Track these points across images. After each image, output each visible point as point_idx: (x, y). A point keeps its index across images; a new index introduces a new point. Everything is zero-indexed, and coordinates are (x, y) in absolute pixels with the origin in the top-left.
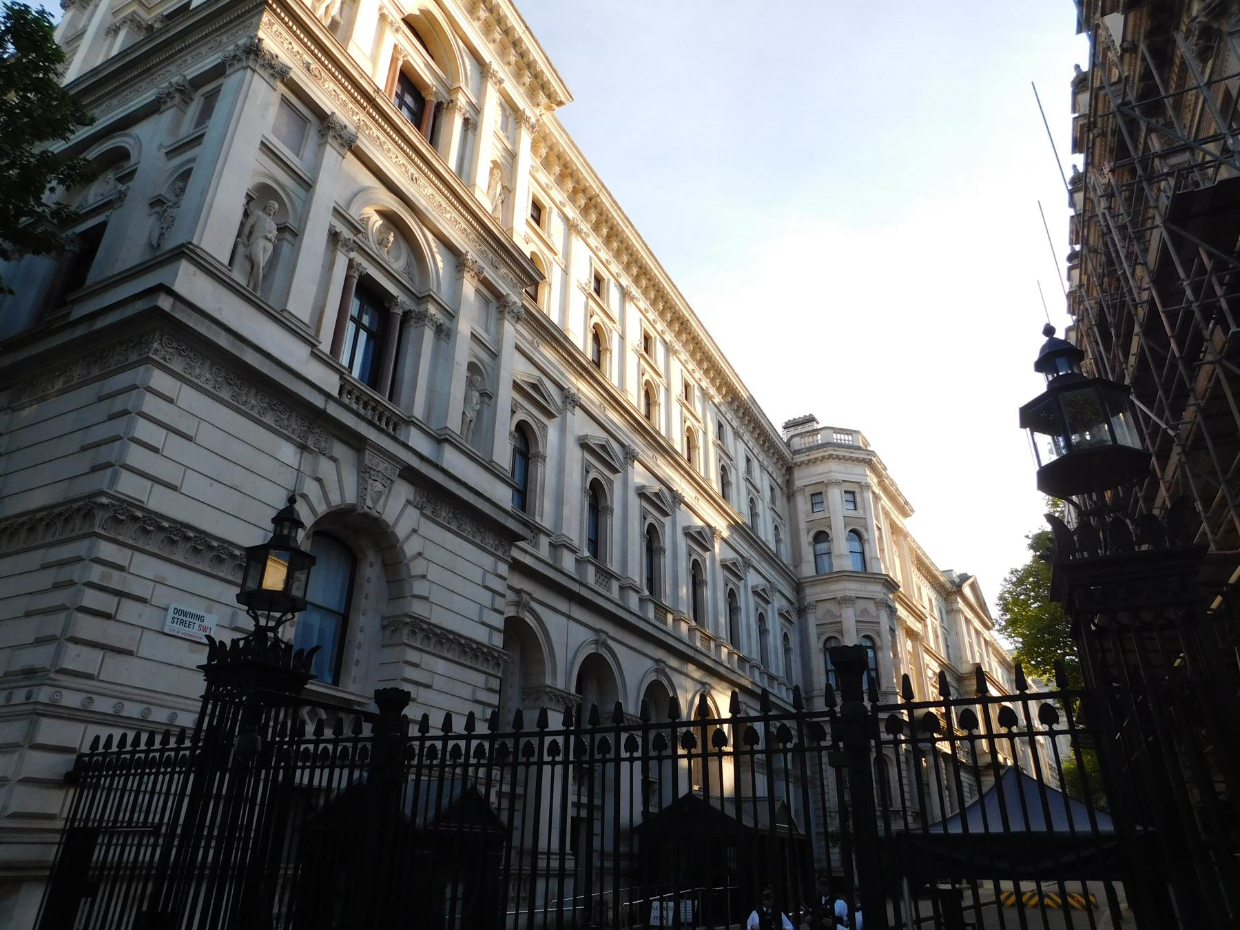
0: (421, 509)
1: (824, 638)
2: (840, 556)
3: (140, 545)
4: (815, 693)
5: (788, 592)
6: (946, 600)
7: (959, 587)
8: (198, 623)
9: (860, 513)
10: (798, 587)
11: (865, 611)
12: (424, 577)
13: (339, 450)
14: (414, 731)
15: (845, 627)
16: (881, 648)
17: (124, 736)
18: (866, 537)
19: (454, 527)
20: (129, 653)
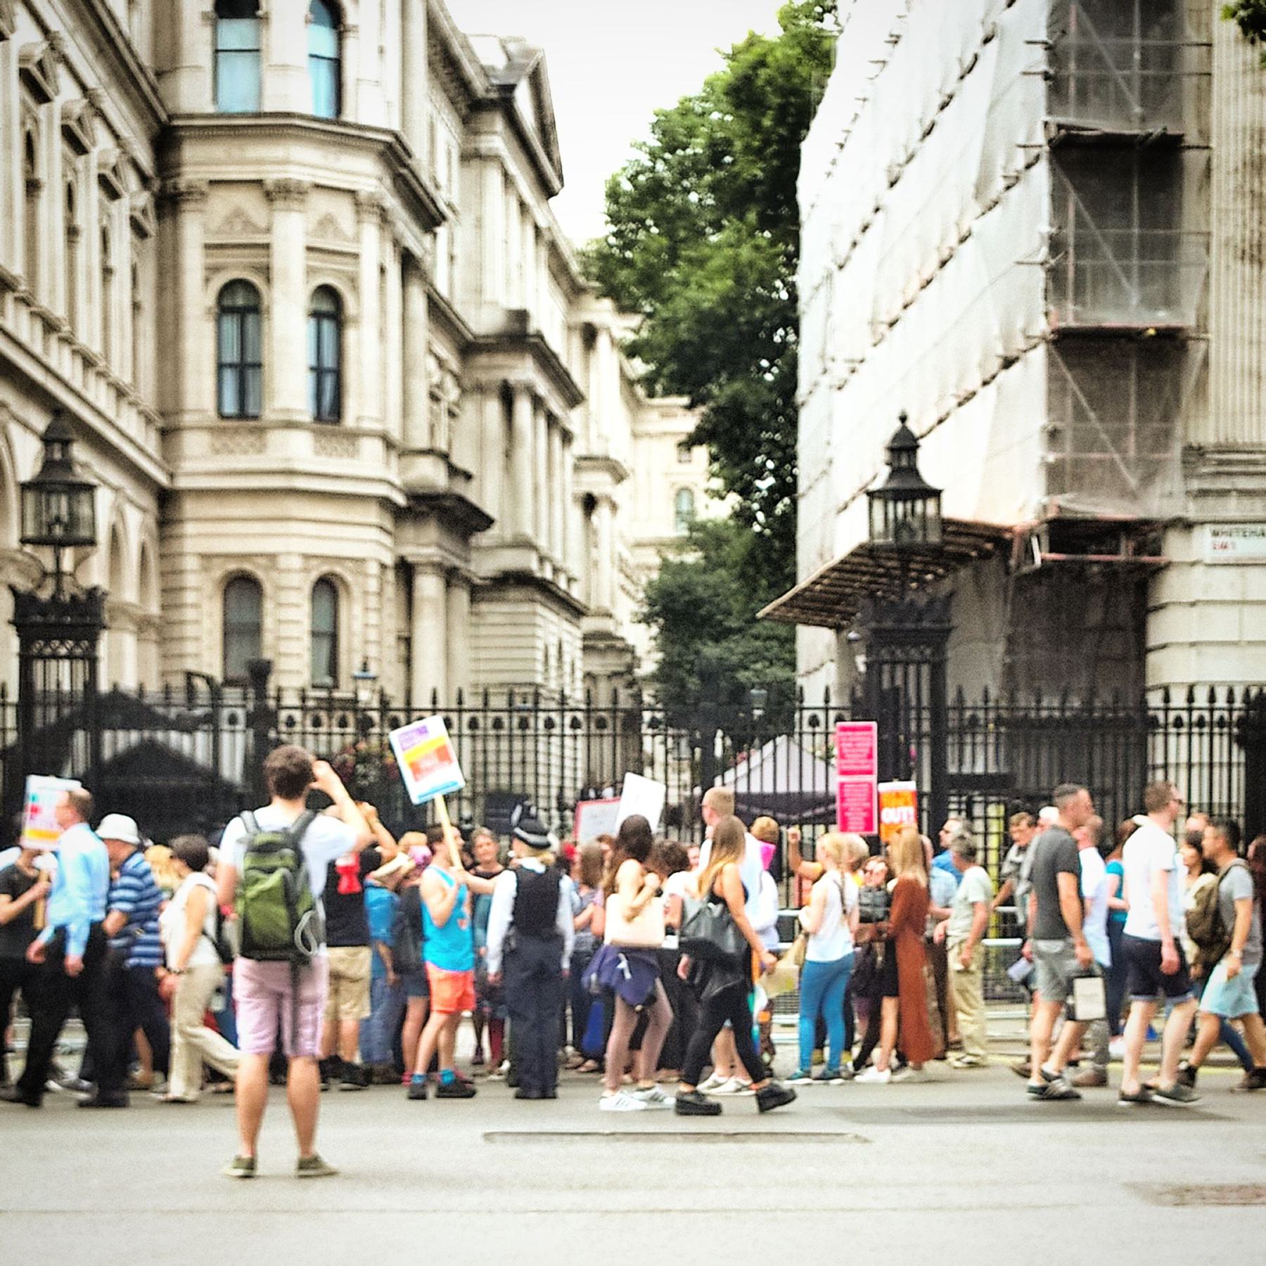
1: (220, 281)
4: (188, 419)
5: (145, 158)
6: (465, 121)
7: (511, 88)
10: (166, 138)
11: (327, 222)
15: (277, 263)
16: (356, 321)
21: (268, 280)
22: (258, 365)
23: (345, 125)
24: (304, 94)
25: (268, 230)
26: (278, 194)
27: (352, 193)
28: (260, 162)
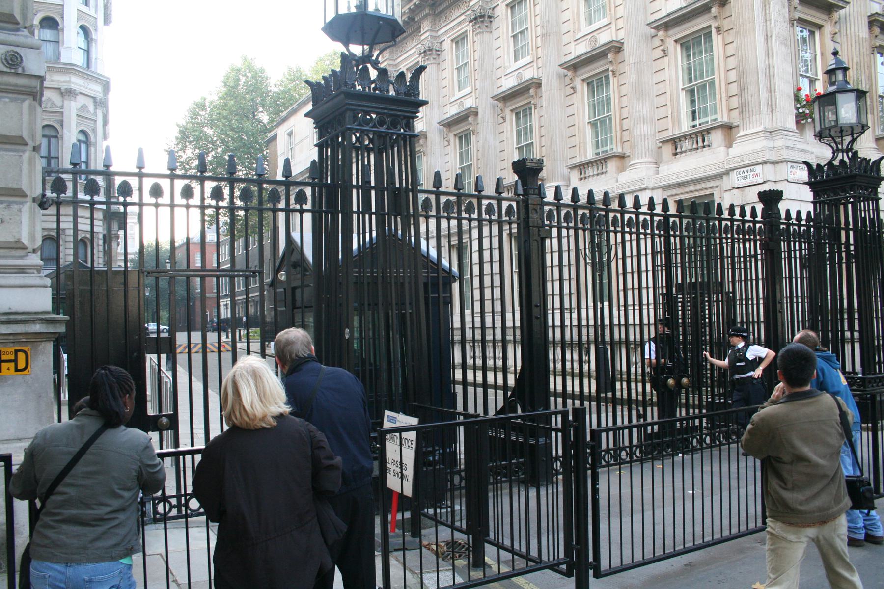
2: (70, 48)
9: (92, 12)
14: (550, 196)
16: (95, 144)
18: (94, 37)
21: (62, 125)
22: (58, 158)
23: (93, 72)
24: (78, 59)
25: (62, 107)
26: (68, 93)
27: (94, 98)
28: (59, 81)
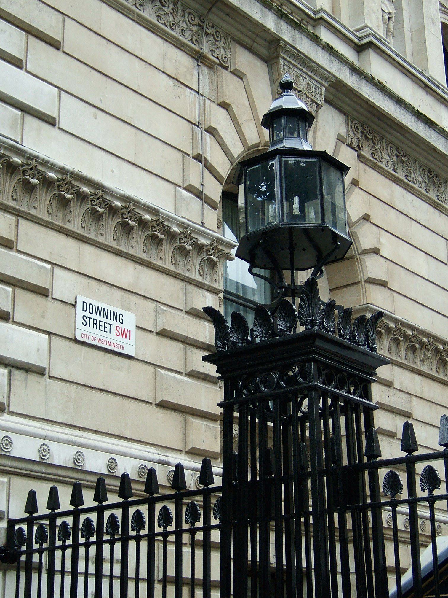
0: (358, 149)
3: (24, 208)
8: (115, 324)
12: (376, 251)
13: (244, 60)
17: (53, 494)
19: (400, 175)
20: (40, 372)
